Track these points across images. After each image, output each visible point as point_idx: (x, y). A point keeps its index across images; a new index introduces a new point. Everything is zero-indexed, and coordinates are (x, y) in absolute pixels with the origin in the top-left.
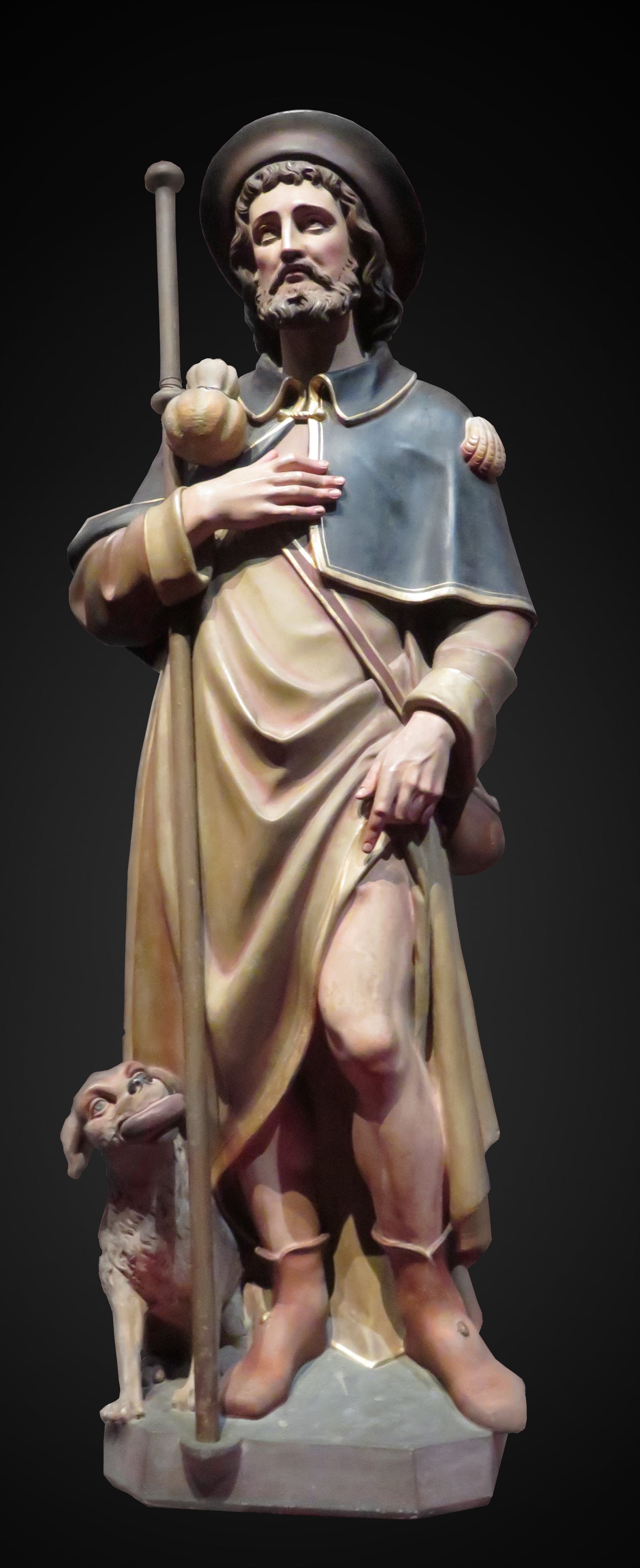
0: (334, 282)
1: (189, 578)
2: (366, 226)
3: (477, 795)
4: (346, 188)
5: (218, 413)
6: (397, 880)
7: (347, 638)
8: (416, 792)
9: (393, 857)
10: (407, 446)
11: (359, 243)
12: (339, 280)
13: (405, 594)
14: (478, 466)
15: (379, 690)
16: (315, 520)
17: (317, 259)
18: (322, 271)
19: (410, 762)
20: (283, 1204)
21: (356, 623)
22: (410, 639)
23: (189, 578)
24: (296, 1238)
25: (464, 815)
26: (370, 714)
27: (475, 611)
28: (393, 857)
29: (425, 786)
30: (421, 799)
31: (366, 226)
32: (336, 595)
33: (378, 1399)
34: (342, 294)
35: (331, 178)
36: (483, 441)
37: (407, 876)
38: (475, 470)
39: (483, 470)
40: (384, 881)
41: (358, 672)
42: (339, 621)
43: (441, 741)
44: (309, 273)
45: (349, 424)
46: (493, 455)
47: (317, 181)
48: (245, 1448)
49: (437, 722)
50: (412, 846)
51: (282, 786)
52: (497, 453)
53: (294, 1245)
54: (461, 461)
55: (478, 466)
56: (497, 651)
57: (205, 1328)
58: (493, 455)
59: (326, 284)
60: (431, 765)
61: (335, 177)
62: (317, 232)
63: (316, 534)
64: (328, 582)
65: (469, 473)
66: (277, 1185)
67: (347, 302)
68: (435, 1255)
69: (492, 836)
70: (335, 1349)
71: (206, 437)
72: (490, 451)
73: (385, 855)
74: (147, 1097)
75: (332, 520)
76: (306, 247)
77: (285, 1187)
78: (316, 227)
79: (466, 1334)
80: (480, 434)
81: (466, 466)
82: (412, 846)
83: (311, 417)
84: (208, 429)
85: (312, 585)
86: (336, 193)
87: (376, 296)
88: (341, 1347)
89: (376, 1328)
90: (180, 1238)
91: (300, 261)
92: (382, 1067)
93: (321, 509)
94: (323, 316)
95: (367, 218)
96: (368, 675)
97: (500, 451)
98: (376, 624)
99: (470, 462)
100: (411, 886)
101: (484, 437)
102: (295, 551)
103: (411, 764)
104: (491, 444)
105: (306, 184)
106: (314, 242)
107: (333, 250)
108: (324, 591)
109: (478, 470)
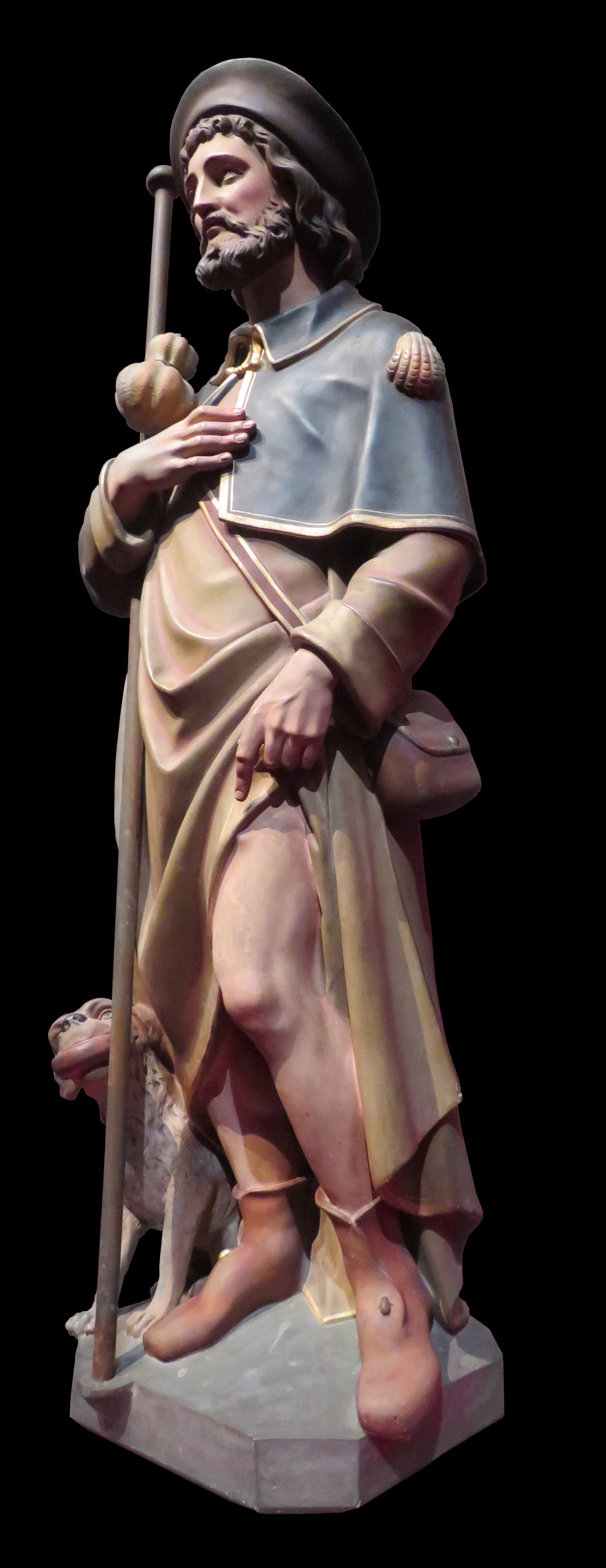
0: (249, 228)
1: (118, 545)
2: (287, 163)
3: (401, 733)
4: (258, 129)
5: (143, 381)
6: (287, 827)
7: (252, 581)
8: (279, 733)
9: (285, 803)
10: (333, 377)
11: (283, 181)
12: (257, 224)
13: (300, 528)
14: (403, 383)
15: (283, 631)
16: (228, 467)
17: (232, 209)
18: (234, 219)
19: (274, 703)
20: (245, 1146)
21: (259, 565)
22: (332, 576)
23: (118, 545)
24: (260, 1179)
25: (386, 756)
26: (273, 658)
27: (391, 537)
28: (285, 803)
29: (291, 727)
30: (289, 742)
31: (287, 163)
32: (241, 540)
33: (293, 1364)
34: (257, 237)
35: (238, 122)
36: (406, 356)
37: (302, 823)
38: (401, 388)
39: (409, 387)
40: (268, 829)
41: (263, 615)
42: (241, 565)
43: (309, 679)
44: (222, 223)
45: (278, 367)
46: (418, 368)
47: (226, 129)
48: (135, 1391)
49: (305, 657)
50: (303, 792)
51: (184, 735)
52: (433, 366)
53: (258, 1187)
54: (387, 381)
55: (403, 383)
56: (416, 579)
57: (104, 1266)
58: (418, 368)
59: (241, 231)
60: (297, 705)
61: (243, 120)
62: (231, 181)
63: (226, 483)
64: (233, 529)
65: (395, 393)
66: (238, 1128)
67: (262, 245)
68: (359, 1221)
69: (418, 777)
70: (304, 1294)
71: (138, 407)
72: (413, 364)
73: (274, 800)
74: (74, 1036)
75: (245, 467)
76: (219, 199)
77: (245, 1131)
78: (229, 176)
79: (386, 1313)
80: (413, 348)
81: (393, 384)
82: (303, 792)
83: (248, 369)
84: (137, 399)
85: (218, 533)
86: (248, 138)
87: (315, 233)
88: (308, 1294)
89: (339, 1283)
90: (148, 1168)
91: (213, 214)
92: (253, 1024)
93: (227, 455)
94: (233, 263)
95: (288, 154)
96: (273, 618)
97: (435, 362)
98: (294, 564)
99: (395, 381)
100: (307, 834)
101: (407, 351)
102: (208, 502)
103: (275, 706)
104: (415, 357)
105: (218, 136)
106: (228, 192)
107: (249, 197)
108: (230, 538)
109: (410, 387)
